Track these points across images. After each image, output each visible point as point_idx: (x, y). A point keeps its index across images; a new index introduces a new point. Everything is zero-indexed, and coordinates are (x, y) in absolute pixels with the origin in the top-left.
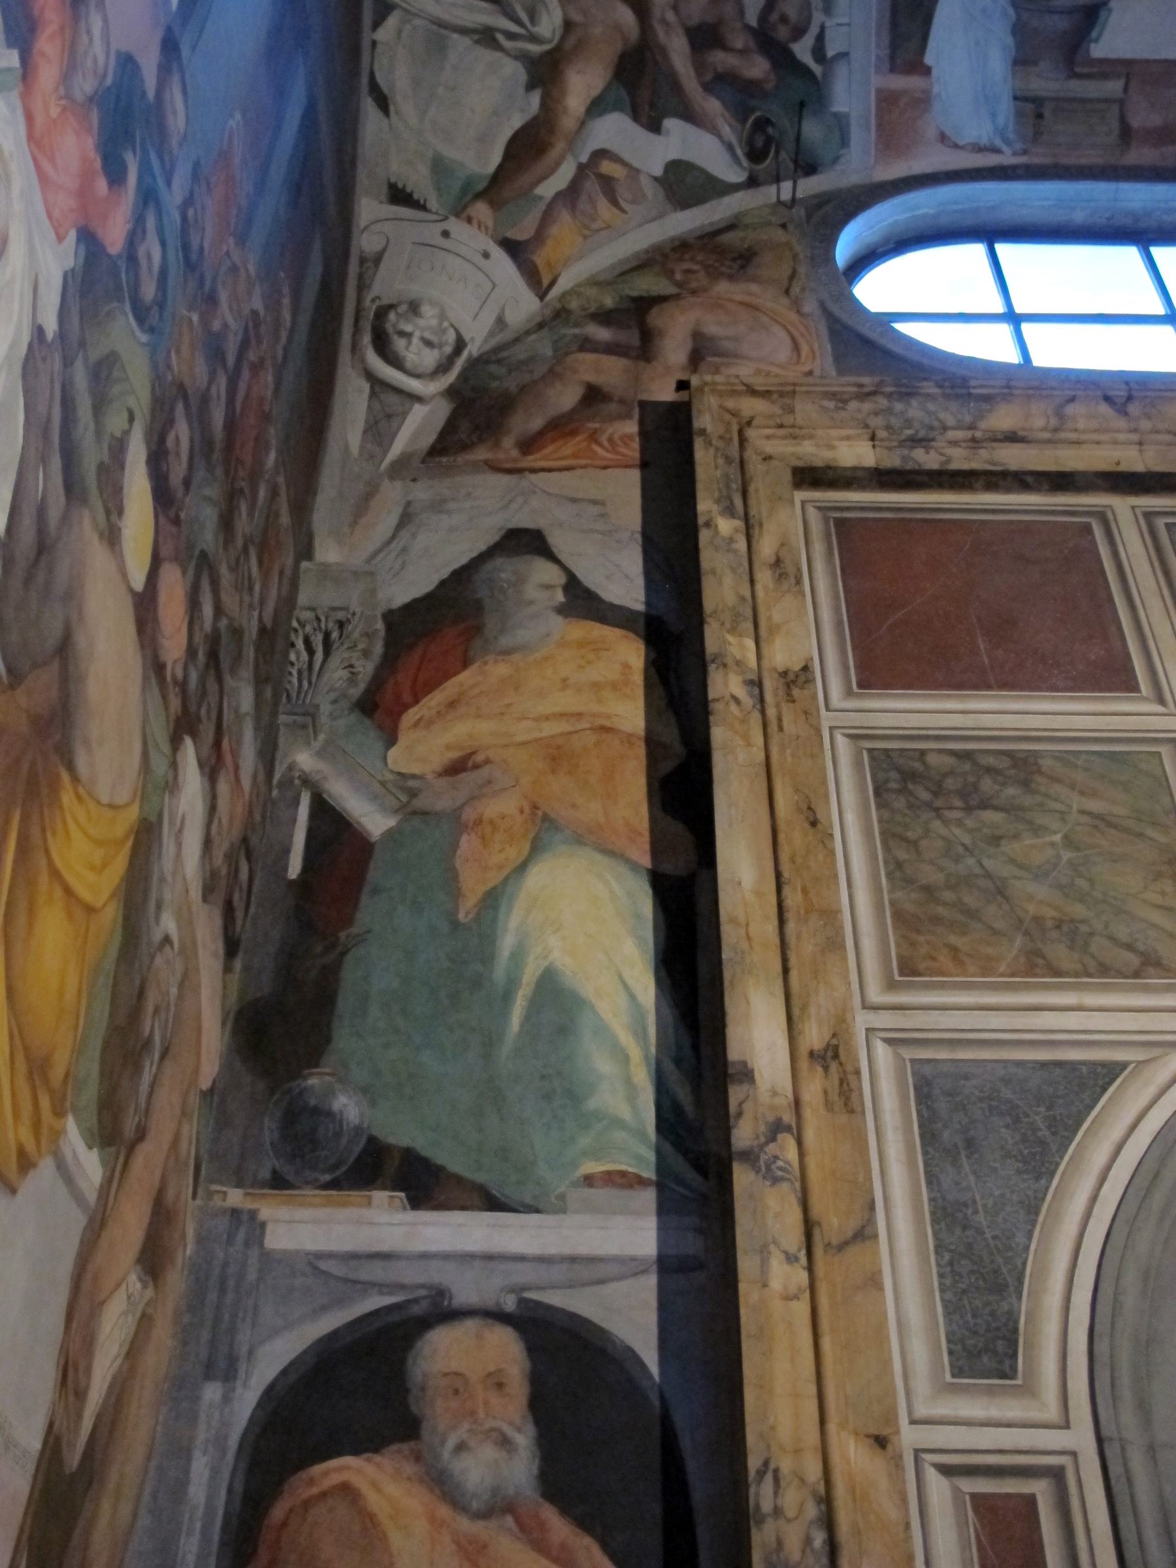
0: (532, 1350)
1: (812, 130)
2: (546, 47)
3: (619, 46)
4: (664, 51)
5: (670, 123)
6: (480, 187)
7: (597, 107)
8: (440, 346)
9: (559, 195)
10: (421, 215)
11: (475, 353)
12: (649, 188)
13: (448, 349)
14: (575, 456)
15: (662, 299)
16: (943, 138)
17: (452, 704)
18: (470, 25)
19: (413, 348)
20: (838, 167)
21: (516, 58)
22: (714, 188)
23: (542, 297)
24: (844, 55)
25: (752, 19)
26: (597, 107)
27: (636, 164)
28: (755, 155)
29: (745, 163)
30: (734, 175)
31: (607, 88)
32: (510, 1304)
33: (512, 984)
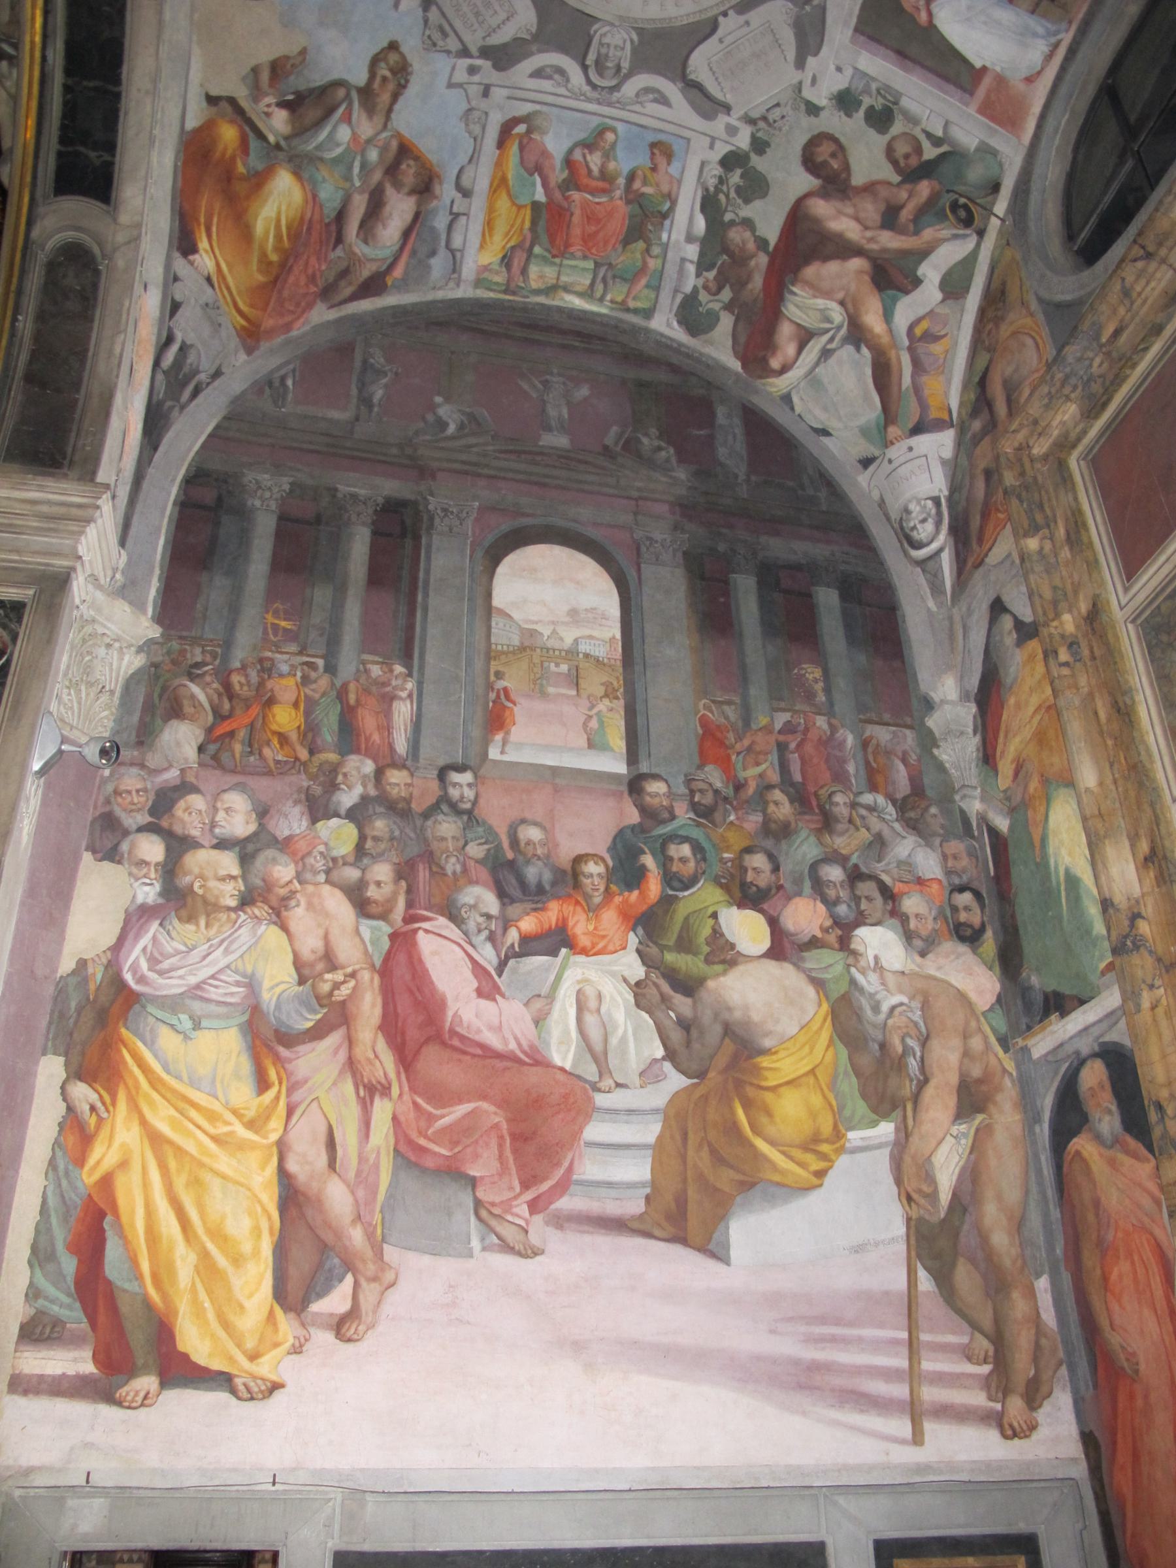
0: (1108, 1066)
1: (975, 174)
2: (846, 324)
3: (867, 278)
4: (885, 250)
5: (920, 272)
6: (882, 422)
7: (888, 315)
8: (929, 515)
9: (914, 375)
10: (878, 462)
11: (946, 493)
12: (944, 310)
13: (934, 511)
14: (995, 529)
15: (987, 369)
16: (1029, 80)
17: (1006, 736)
18: (816, 359)
19: (921, 530)
20: (1006, 166)
21: (842, 346)
22: (969, 262)
23: (952, 426)
24: (947, 125)
25: (896, 179)
26: (888, 315)
27: (928, 310)
28: (968, 222)
29: (968, 232)
30: (970, 244)
31: (882, 300)
32: (1097, 1048)
33: (1058, 884)
